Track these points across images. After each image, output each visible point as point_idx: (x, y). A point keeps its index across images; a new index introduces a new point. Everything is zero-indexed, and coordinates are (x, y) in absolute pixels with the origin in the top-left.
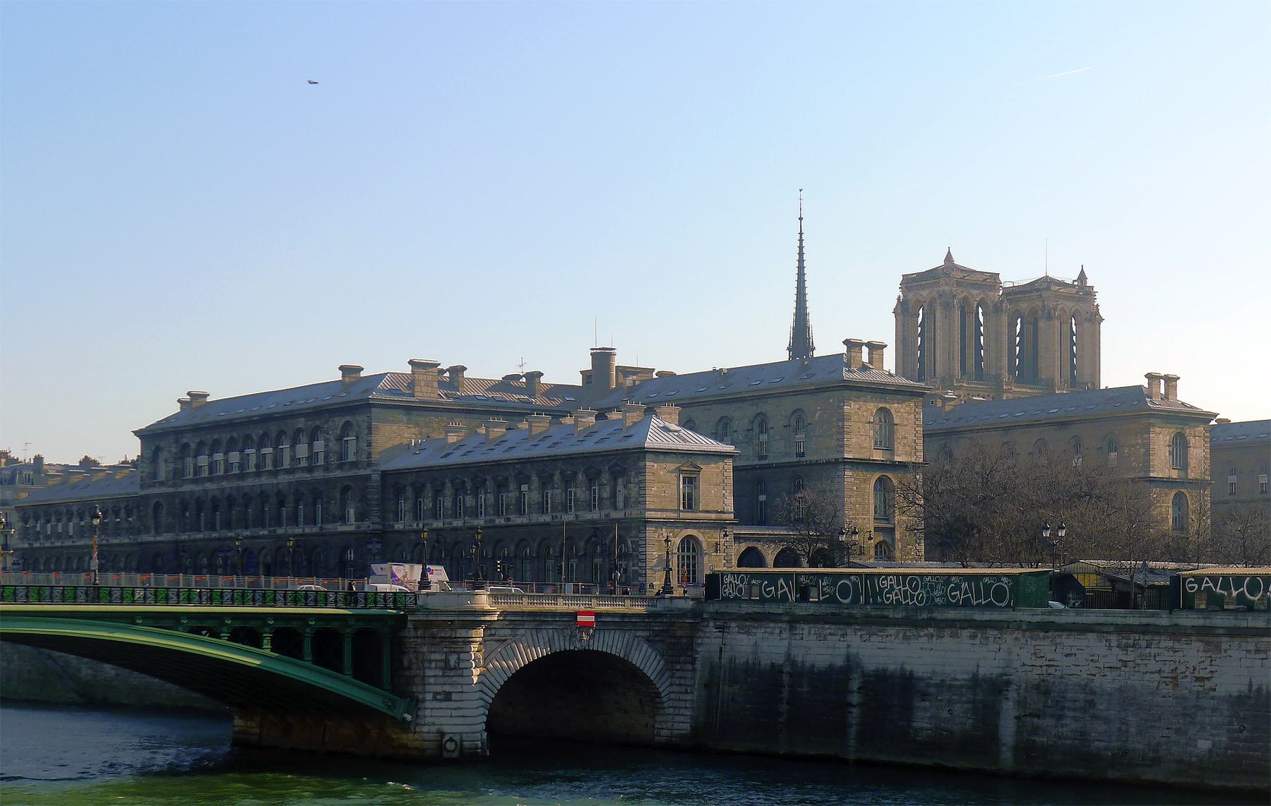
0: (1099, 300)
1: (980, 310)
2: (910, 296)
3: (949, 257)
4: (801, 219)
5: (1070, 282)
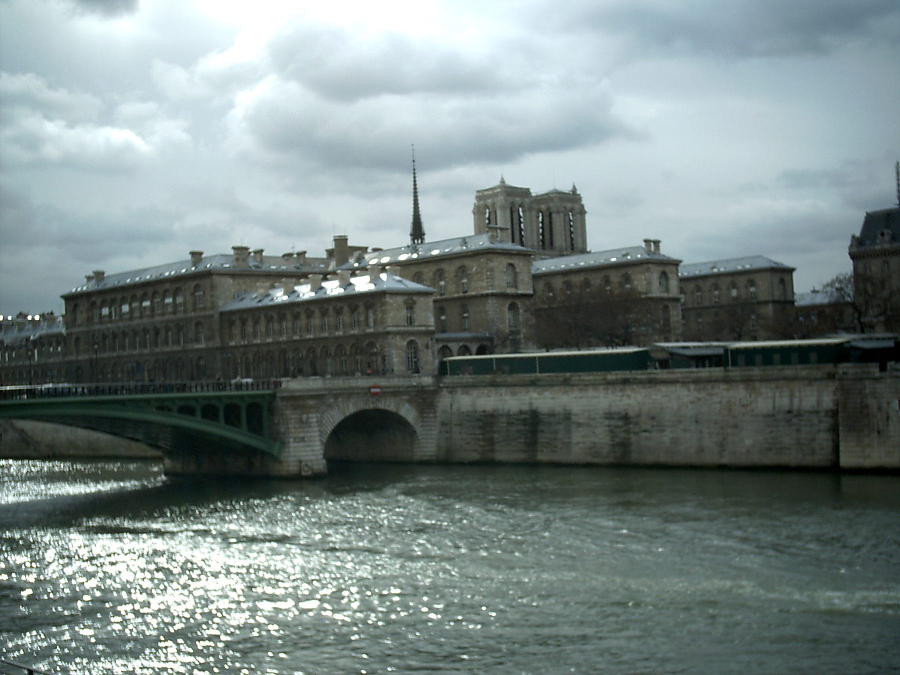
0: (584, 202)
1: (520, 209)
2: (481, 202)
3: (503, 182)
4: (414, 161)
5: (567, 192)
